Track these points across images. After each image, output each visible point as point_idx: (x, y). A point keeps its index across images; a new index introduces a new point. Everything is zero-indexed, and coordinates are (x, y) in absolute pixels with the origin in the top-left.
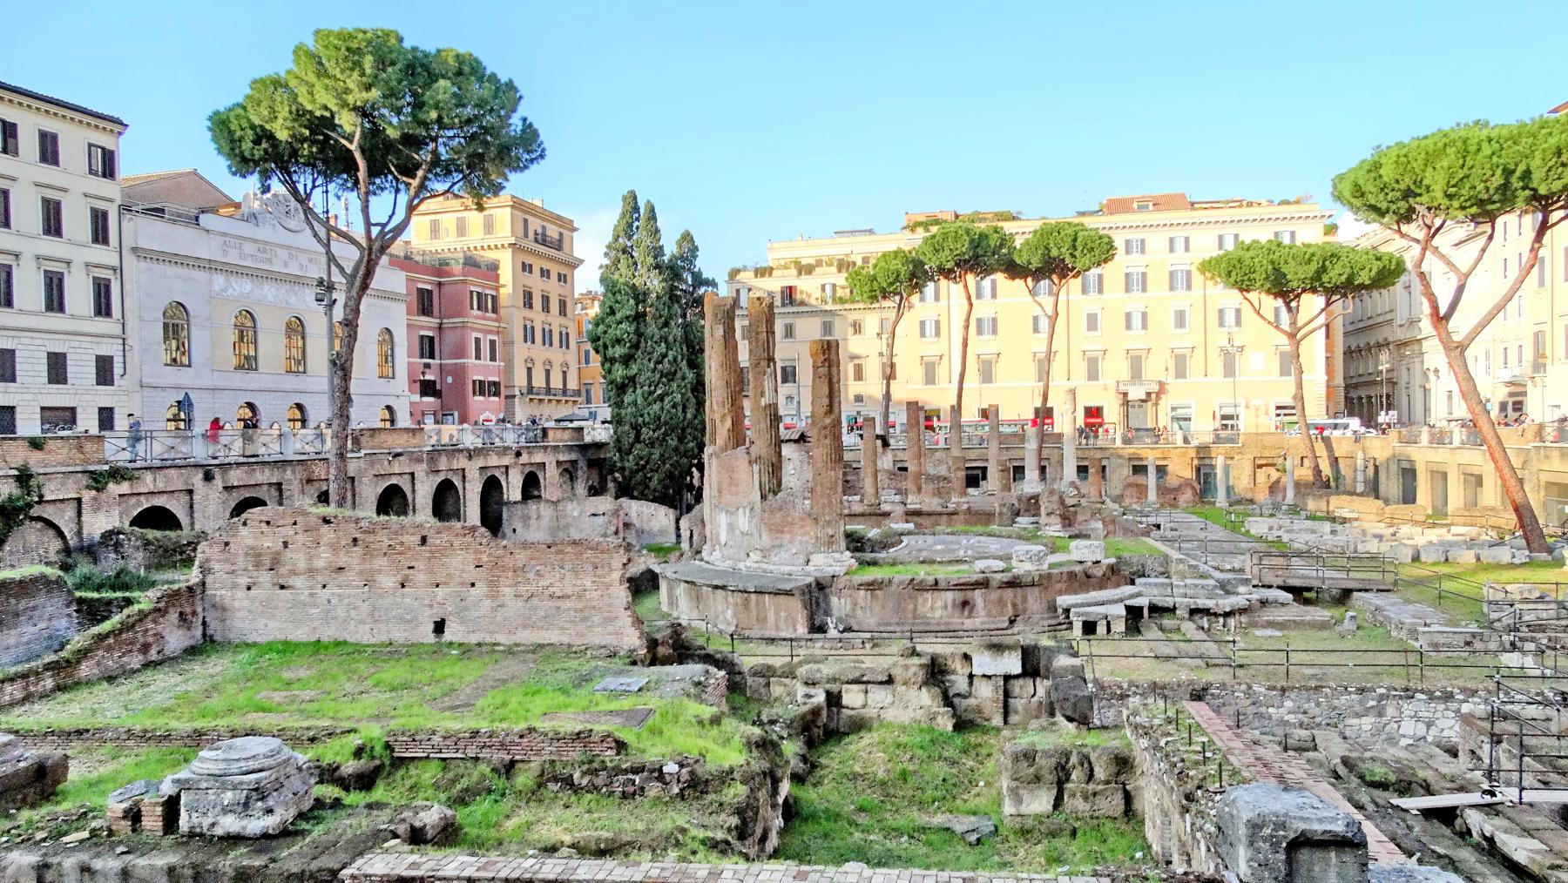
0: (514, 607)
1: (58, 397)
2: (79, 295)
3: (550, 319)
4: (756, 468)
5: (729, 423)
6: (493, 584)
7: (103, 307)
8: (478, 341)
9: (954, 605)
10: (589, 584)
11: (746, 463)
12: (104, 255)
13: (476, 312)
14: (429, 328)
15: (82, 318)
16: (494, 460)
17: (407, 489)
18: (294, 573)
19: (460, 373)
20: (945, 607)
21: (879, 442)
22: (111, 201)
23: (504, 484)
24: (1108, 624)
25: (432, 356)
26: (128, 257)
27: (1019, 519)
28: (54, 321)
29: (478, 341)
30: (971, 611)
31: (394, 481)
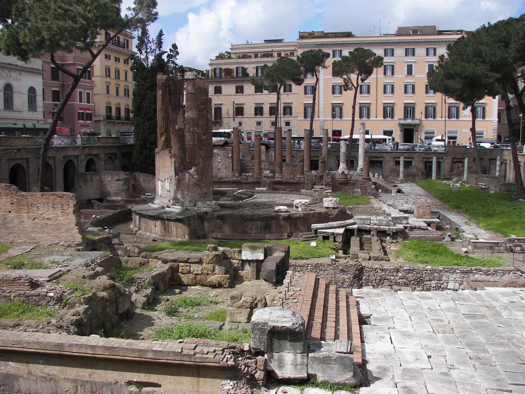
0: (28, 223)
3: (119, 82)
4: (173, 160)
5: (163, 138)
6: (18, 212)
8: (81, 93)
9: (261, 227)
10: (60, 213)
11: (169, 158)
16: (71, 153)
17: (25, 166)
20: (257, 228)
21: (263, 148)
23: (76, 164)
29: (81, 93)
30: (270, 230)
31: (18, 162)
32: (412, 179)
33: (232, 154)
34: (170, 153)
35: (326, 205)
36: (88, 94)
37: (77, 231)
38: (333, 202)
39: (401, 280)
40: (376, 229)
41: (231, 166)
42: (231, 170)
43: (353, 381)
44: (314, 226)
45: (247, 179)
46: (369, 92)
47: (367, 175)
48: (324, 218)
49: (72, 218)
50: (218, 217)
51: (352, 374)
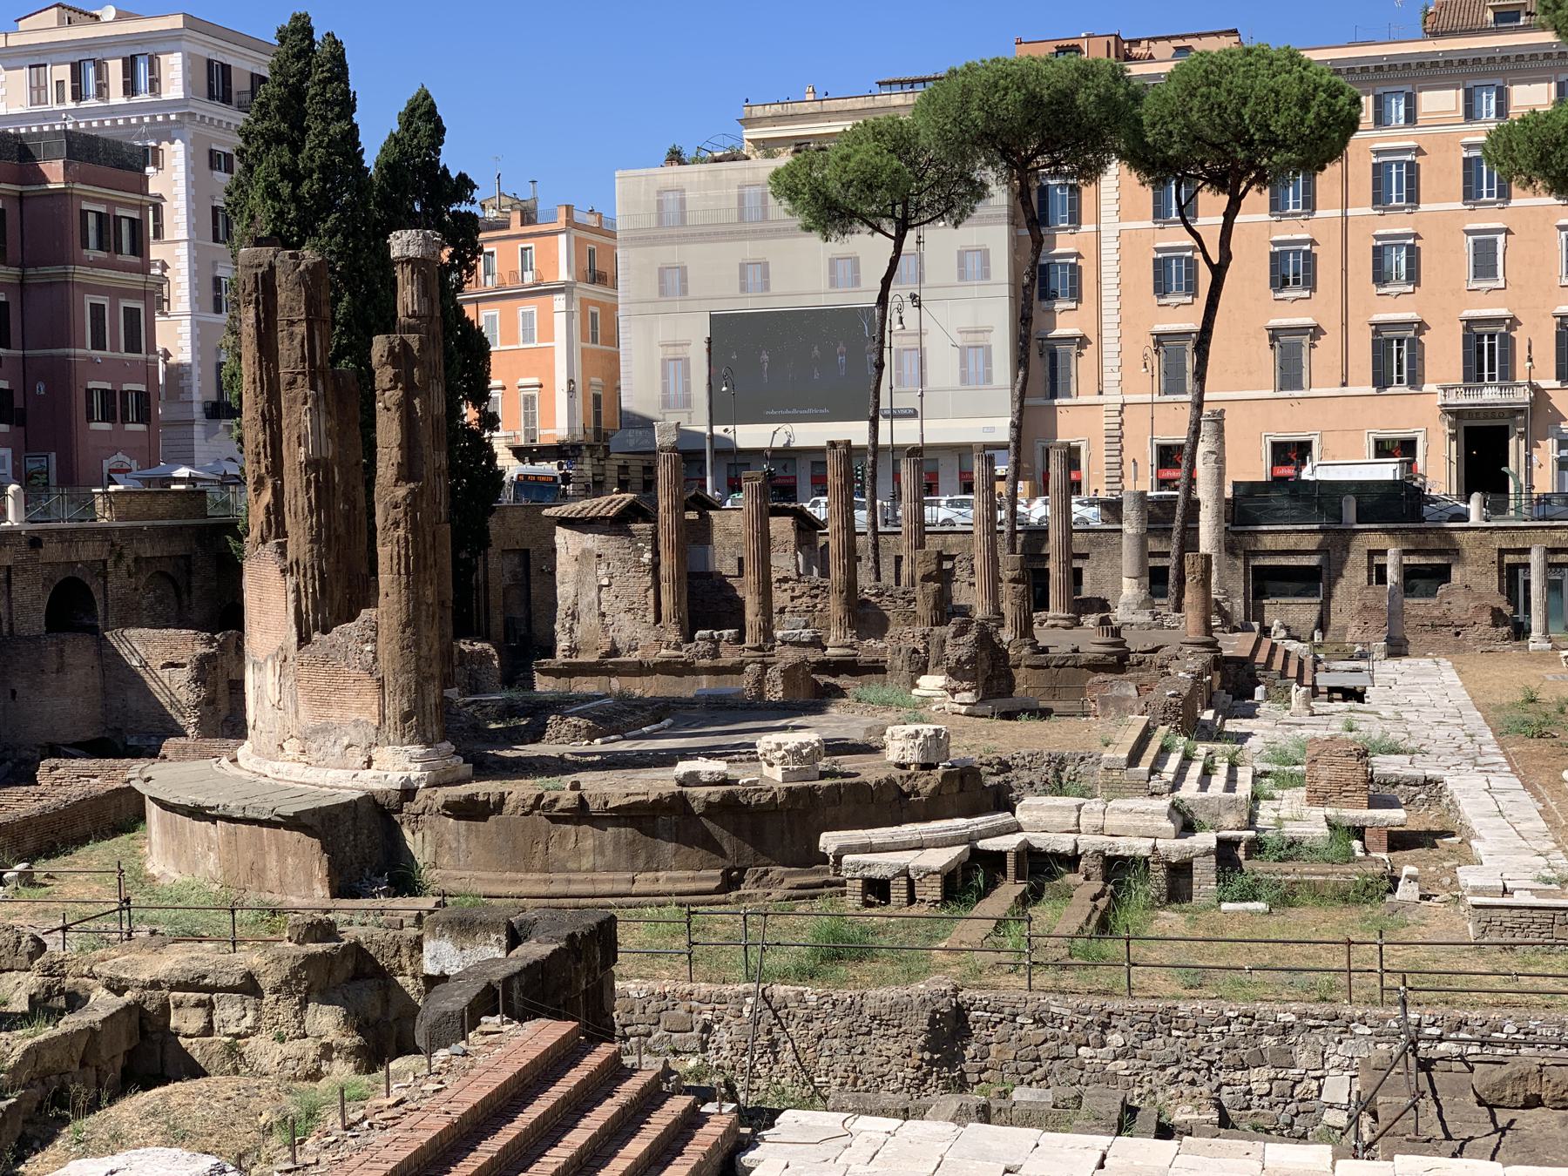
4: (291, 581)
8: (97, 310)
11: (278, 574)
13: (93, 253)
19: (61, 374)
24: (911, 883)
27: (924, 681)
29: (97, 310)
32: (1452, 640)
33: (656, 553)
34: (283, 555)
35: (893, 754)
36: (132, 315)
38: (921, 739)
39: (1122, 1063)
40: (1102, 853)
41: (651, 602)
42: (651, 617)
44: (829, 841)
45: (716, 654)
46: (1310, 283)
47: (1201, 626)
48: (888, 804)
50: (446, 806)
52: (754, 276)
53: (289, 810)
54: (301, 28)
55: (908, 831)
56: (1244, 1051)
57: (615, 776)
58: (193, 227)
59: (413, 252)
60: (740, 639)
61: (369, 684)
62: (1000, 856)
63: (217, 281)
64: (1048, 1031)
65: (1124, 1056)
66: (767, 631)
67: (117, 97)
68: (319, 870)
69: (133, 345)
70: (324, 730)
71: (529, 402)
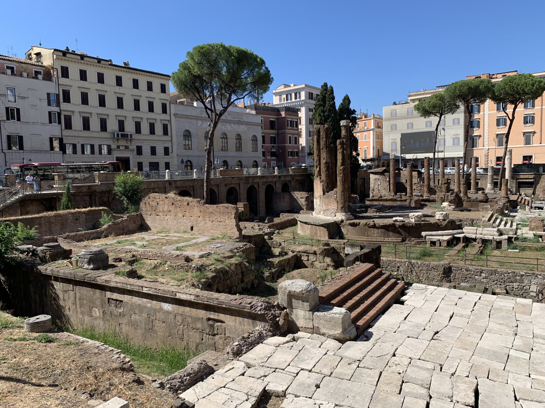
1: (154, 159)
2: (159, 129)
4: (322, 184)
7: (166, 132)
8: (290, 137)
12: (165, 117)
13: (289, 127)
14: (274, 134)
15: (160, 136)
17: (237, 188)
18: (160, 211)
19: (284, 148)
22: (167, 100)
23: (274, 187)
25: (275, 144)
26: (173, 117)
27: (444, 203)
28: (152, 137)
29: (290, 137)
33: (390, 178)
35: (437, 217)
36: (296, 138)
37: (236, 229)
39: (485, 280)
43: (342, 336)
44: (423, 234)
45: (401, 198)
48: (436, 227)
49: (233, 222)
51: (341, 330)
52: (410, 126)
53: (321, 224)
54: (326, 85)
55: (440, 232)
56: (512, 279)
57: (381, 220)
58: (306, 122)
59: (345, 124)
60: (406, 195)
61: (336, 202)
62: (460, 238)
63: (310, 131)
64: (469, 273)
65: (485, 278)
66: (411, 193)
67: (293, 100)
68: (327, 234)
69: (296, 143)
70: (327, 210)
71: (365, 151)
